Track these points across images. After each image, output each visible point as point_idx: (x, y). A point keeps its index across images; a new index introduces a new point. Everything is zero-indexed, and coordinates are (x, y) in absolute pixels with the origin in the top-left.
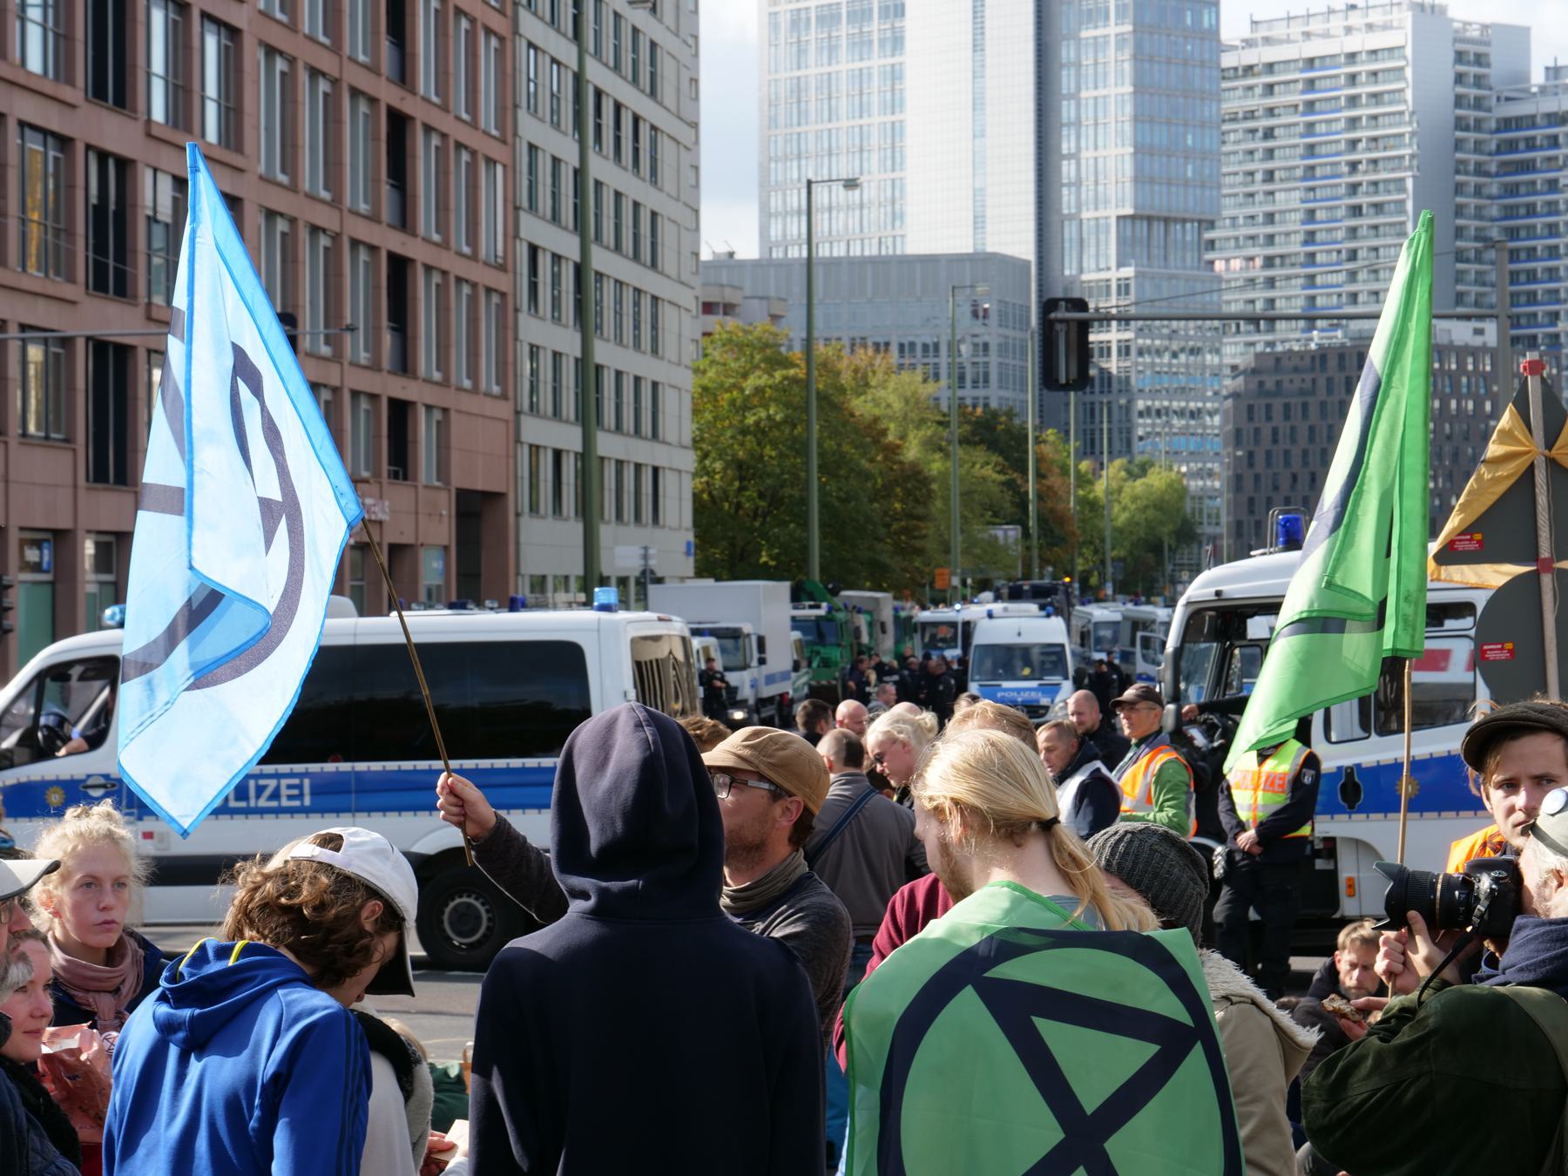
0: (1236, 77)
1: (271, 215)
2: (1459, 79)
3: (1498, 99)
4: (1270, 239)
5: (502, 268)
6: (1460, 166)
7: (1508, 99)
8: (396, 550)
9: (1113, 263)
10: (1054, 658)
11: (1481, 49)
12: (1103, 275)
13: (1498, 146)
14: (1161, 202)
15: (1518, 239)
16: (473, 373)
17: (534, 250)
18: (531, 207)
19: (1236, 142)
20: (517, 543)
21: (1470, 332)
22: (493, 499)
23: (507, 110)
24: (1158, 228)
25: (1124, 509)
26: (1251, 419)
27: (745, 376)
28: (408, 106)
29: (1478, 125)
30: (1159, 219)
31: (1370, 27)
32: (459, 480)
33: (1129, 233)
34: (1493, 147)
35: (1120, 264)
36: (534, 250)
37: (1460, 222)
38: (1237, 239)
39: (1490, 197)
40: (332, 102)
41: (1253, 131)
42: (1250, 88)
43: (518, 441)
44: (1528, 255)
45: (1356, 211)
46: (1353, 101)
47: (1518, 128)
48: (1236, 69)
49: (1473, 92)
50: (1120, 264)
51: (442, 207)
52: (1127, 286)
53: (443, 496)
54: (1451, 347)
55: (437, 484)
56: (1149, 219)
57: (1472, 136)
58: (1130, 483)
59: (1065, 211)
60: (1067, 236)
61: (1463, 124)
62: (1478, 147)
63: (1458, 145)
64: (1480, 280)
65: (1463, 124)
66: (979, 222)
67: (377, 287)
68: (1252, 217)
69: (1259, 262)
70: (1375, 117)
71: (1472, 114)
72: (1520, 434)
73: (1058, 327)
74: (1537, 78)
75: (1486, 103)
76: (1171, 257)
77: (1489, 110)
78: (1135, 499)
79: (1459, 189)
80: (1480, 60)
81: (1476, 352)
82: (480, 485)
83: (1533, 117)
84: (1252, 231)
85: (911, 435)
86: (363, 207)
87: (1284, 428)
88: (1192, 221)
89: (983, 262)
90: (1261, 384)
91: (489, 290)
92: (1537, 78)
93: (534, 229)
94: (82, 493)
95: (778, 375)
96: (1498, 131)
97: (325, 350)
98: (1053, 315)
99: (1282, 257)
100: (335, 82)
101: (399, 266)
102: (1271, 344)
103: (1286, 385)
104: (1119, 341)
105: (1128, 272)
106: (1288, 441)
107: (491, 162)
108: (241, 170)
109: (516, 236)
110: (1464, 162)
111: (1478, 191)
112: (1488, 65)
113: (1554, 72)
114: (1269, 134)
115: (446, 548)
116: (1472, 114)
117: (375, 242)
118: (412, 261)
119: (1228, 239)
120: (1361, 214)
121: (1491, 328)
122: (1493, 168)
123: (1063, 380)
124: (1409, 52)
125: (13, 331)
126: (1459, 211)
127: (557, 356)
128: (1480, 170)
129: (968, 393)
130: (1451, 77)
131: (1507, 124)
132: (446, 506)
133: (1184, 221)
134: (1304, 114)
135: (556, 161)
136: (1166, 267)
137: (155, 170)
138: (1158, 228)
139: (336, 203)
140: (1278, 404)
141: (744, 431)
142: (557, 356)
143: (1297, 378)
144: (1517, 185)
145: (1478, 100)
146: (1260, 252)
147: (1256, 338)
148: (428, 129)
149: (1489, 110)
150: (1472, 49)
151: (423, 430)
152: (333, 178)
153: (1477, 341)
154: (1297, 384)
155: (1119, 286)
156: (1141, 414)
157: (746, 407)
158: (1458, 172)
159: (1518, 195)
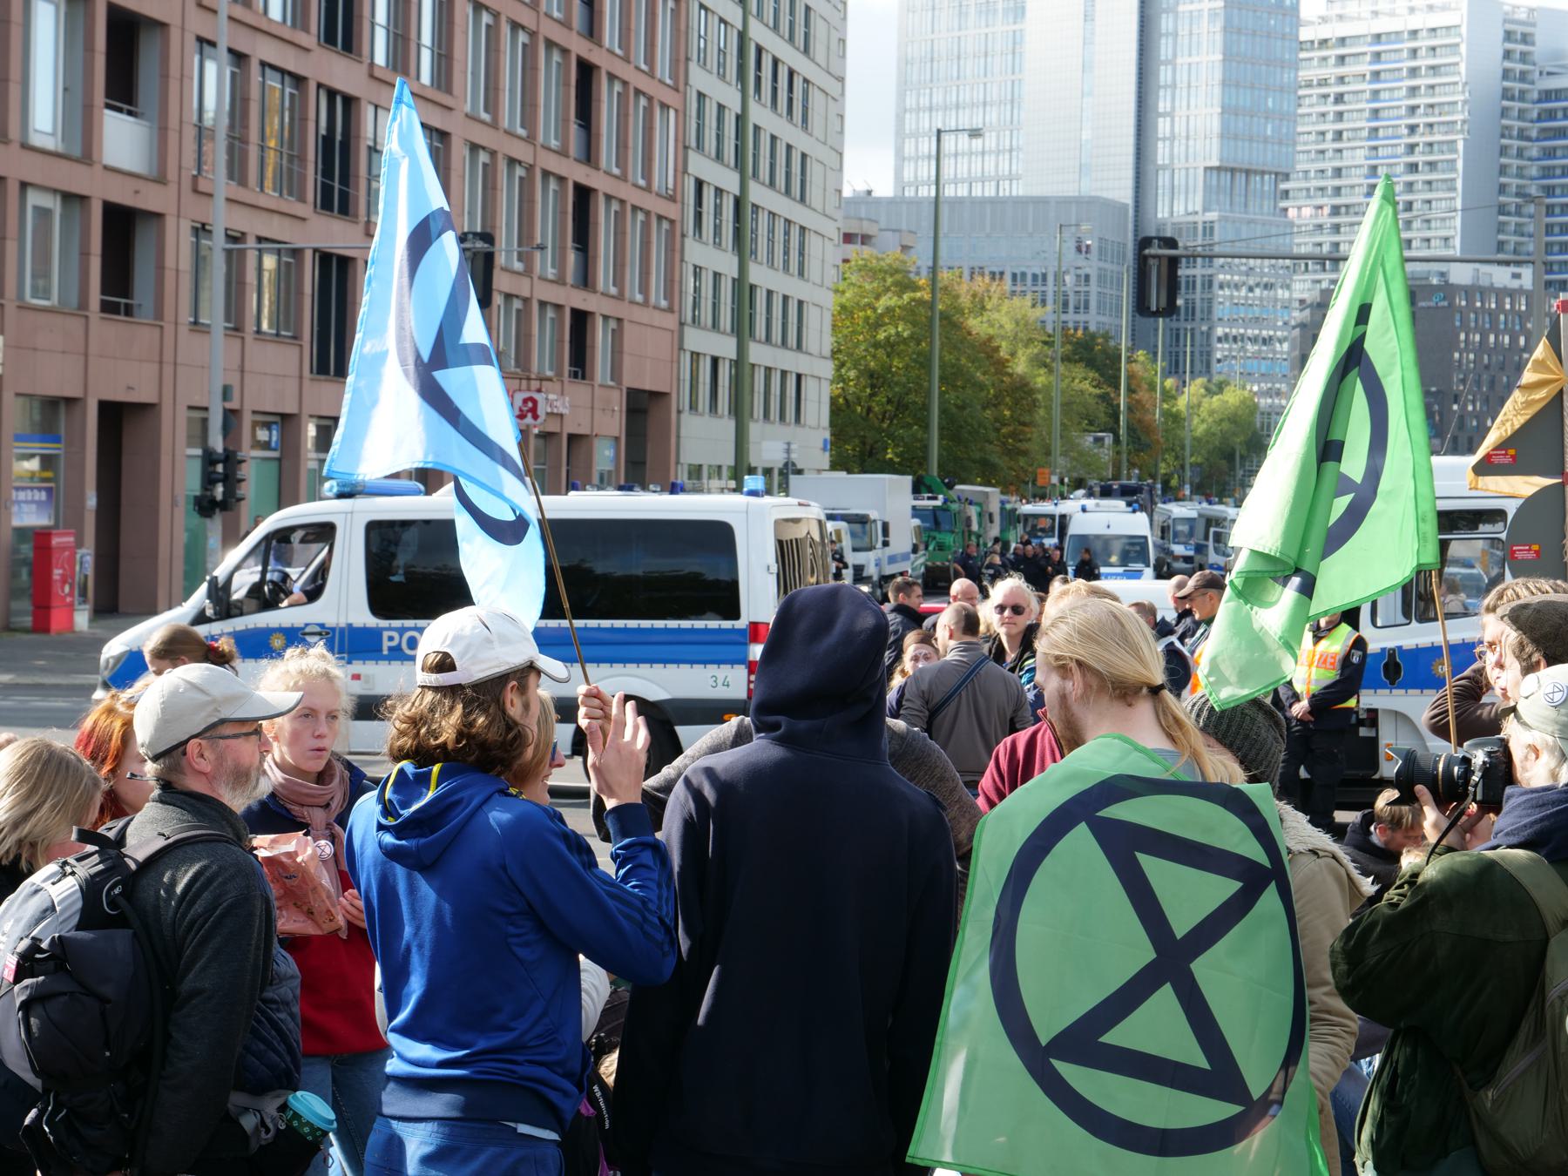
0: (1312, 49)
1: (475, 148)
2: (1507, 55)
3: (1541, 73)
4: (1338, 191)
5: (672, 199)
6: (1505, 132)
7: (1549, 74)
8: (572, 438)
9: (1199, 208)
10: (1138, 548)
12: (1191, 219)
13: (1539, 115)
14: (1245, 156)
15: (1554, 196)
16: (644, 289)
17: (700, 184)
18: (698, 147)
19: (1311, 106)
20: (678, 437)
21: (1510, 275)
22: (657, 396)
23: (680, 63)
24: (1240, 179)
25: (1203, 421)
27: (878, 297)
28: (595, 56)
30: (1241, 170)
32: (629, 381)
33: (1214, 182)
34: (1535, 115)
35: (1205, 209)
36: (700, 184)
37: (1503, 180)
38: (1308, 190)
39: (1530, 159)
40: (529, 52)
41: (1326, 96)
42: (1325, 59)
43: (681, 348)
44: (1562, 210)
45: (1413, 168)
46: (1414, 72)
47: (1557, 100)
48: (1312, 42)
49: (1519, 67)
50: (1205, 209)
51: (622, 145)
52: (1212, 229)
53: (615, 395)
54: (1492, 289)
55: (611, 383)
56: (1233, 171)
57: (1517, 105)
58: (1206, 400)
59: (1160, 162)
61: (1509, 95)
62: (1522, 115)
63: (1504, 113)
64: (1519, 230)
65: (1509, 95)
67: (564, 213)
68: (1322, 171)
69: (1327, 210)
70: (1432, 87)
71: (1517, 86)
72: (1552, 363)
73: (1151, 262)
75: (1529, 77)
76: (1251, 204)
77: (1533, 83)
78: (1211, 413)
79: (1503, 151)
80: (1526, 39)
81: (1512, 294)
82: (648, 385)
84: (1322, 183)
85: (1020, 353)
86: (554, 143)
88: (1270, 173)
91: (660, 218)
93: (700, 166)
94: (306, 383)
95: (906, 297)
96: (1539, 101)
97: (518, 266)
98: (1147, 252)
99: (1347, 206)
100: (533, 34)
101: (583, 195)
104: (1203, 276)
105: (1212, 216)
107: (665, 107)
108: (450, 109)
109: (685, 171)
111: (1520, 154)
112: (1533, 44)
114: (1339, 98)
115: (617, 439)
116: (1517, 86)
117: (563, 173)
118: (595, 190)
119: (1301, 189)
120: (1417, 171)
121: (1527, 273)
122: (1534, 134)
123: (1154, 308)
124: (1464, 30)
125: (251, 243)
126: (1503, 170)
127: (717, 276)
128: (1522, 135)
129: (1070, 317)
130: (1500, 53)
131: (1547, 95)
132: (618, 402)
133: (1263, 173)
134: (1371, 82)
135: (721, 107)
136: (1246, 213)
137: (376, 107)
138: (1240, 179)
139: (530, 139)
141: (877, 345)
142: (717, 276)
144: (1555, 149)
145: (1523, 73)
146: (1329, 201)
148: (612, 77)
149: (1533, 83)
150: (1520, 29)
151: (600, 337)
152: (529, 119)
153: (1515, 284)
155: (1205, 228)
156: (1220, 340)
157: (877, 325)
158: (1503, 136)
159: (1555, 157)
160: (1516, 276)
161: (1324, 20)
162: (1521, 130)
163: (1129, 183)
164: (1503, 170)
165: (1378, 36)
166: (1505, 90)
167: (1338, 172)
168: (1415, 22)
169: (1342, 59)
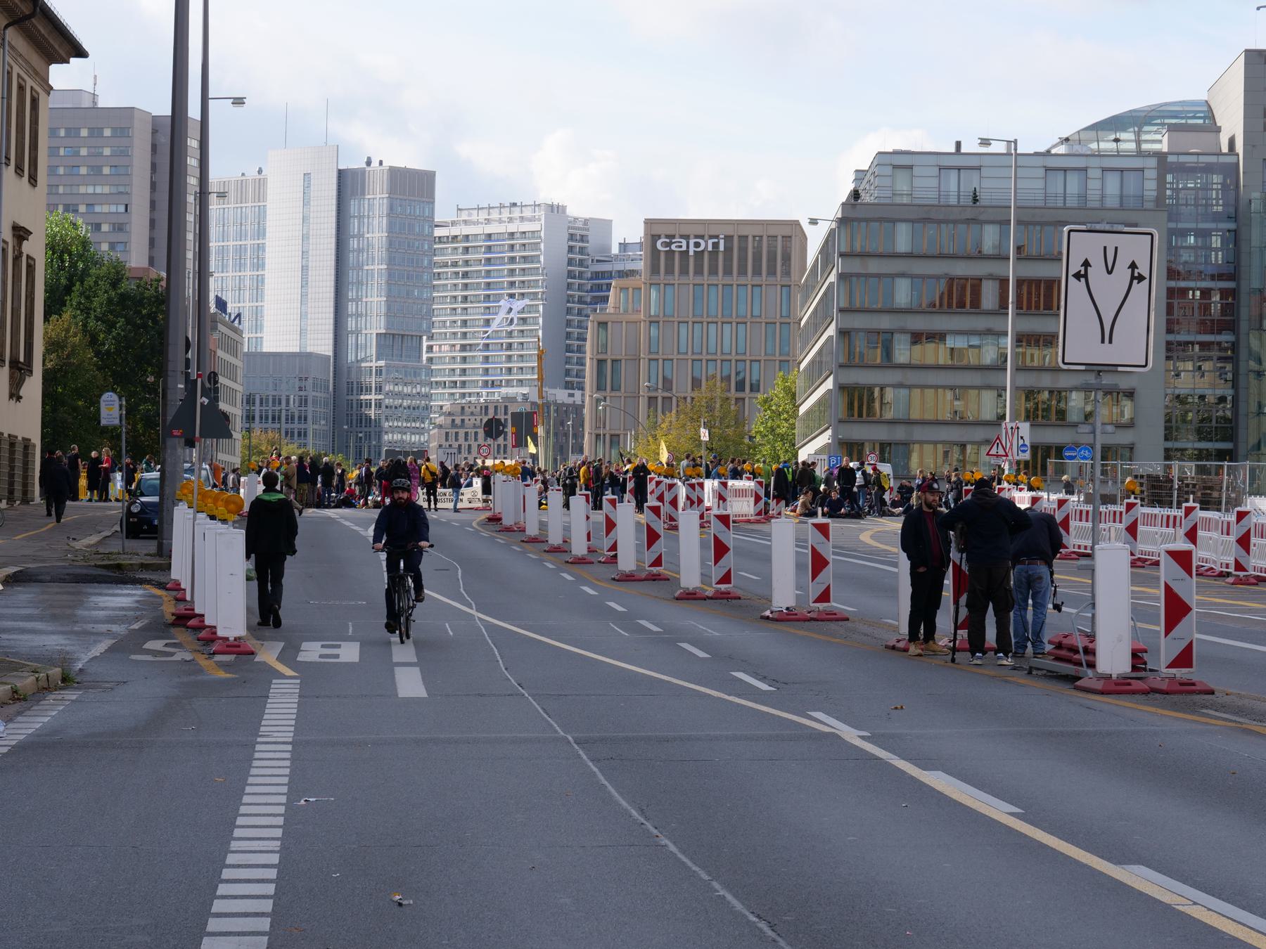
0: (448, 242)
2: (571, 249)
3: (592, 260)
4: (464, 335)
7: (598, 261)
11: (584, 233)
13: (592, 287)
26: (447, 440)
29: (581, 275)
31: (522, 219)
35: (377, 359)
38: (446, 334)
42: (456, 248)
46: (512, 260)
48: (448, 237)
49: (579, 257)
50: (377, 359)
52: (381, 370)
56: (394, 335)
59: (349, 329)
60: (350, 342)
63: (569, 286)
66: (302, 332)
68: (455, 322)
71: (577, 269)
74: (615, 250)
75: (585, 263)
79: (569, 311)
80: (583, 238)
83: (611, 272)
87: (465, 445)
89: (304, 358)
90: (453, 421)
92: (615, 250)
96: (591, 279)
99: (470, 345)
102: (463, 395)
103: (466, 421)
104: (376, 400)
105: (382, 363)
106: (467, 452)
110: (571, 296)
112: (588, 242)
113: (624, 246)
114: (465, 275)
116: (577, 269)
119: (441, 333)
122: (589, 300)
124: (542, 234)
126: (569, 323)
128: (581, 301)
131: (597, 275)
134: (485, 265)
140: (462, 432)
143: (473, 418)
147: (454, 391)
150: (578, 232)
154: (473, 421)
155: (377, 370)
160: (571, 395)
161: (454, 223)
162: (580, 297)
163: (331, 342)
164: (569, 323)
165: (490, 235)
166: (569, 272)
167: (465, 323)
168: (512, 228)
169: (466, 250)
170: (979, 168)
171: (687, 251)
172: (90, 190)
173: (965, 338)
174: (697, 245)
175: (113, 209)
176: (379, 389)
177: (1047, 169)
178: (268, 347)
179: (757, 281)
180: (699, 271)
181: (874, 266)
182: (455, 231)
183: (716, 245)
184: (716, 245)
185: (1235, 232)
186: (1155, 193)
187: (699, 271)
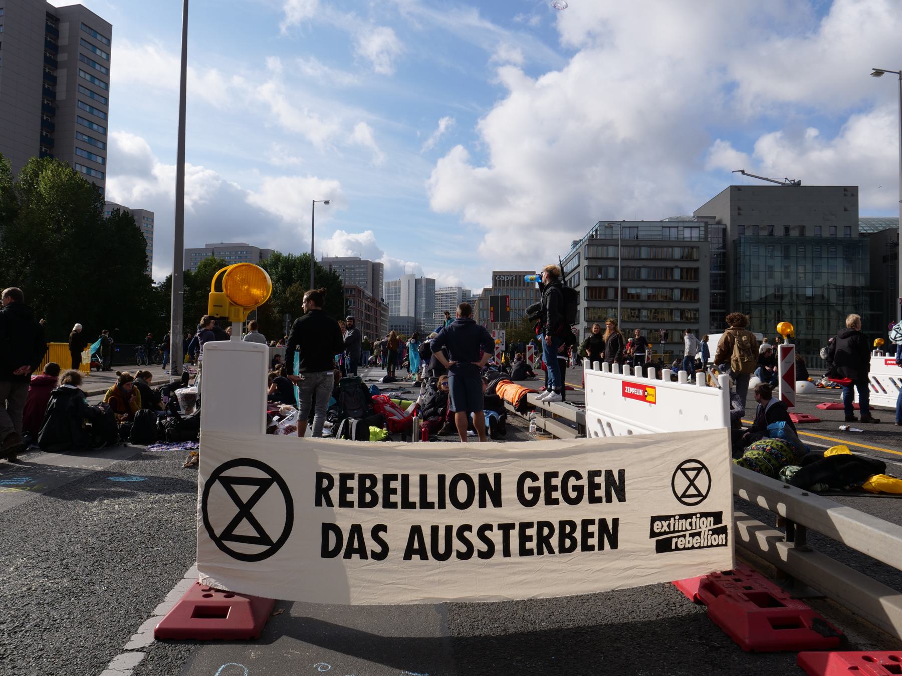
2: (463, 296)
31: (453, 290)
66: (408, 312)
71: (464, 300)
74: (472, 296)
80: (465, 294)
89: (408, 317)
92: (472, 296)
113: (473, 295)
114: (442, 301)
116: (464, 300)
168: (451, 292)
170: (637, 227)
171: (504, 280)
172: (359, 279)
173: (635, 289)
174: (507, 278)
175: (364, 283)
176: (424, 324)
177: (663, 227)
178: (401, 315)
179: (524, 288)
180: (508, 285)
181: (600, 263)
182: (439, 292)
183: (512, 278)
184: (512, 278)
185: (724, 254)
186: (703, 236)
187: (508, 285)
